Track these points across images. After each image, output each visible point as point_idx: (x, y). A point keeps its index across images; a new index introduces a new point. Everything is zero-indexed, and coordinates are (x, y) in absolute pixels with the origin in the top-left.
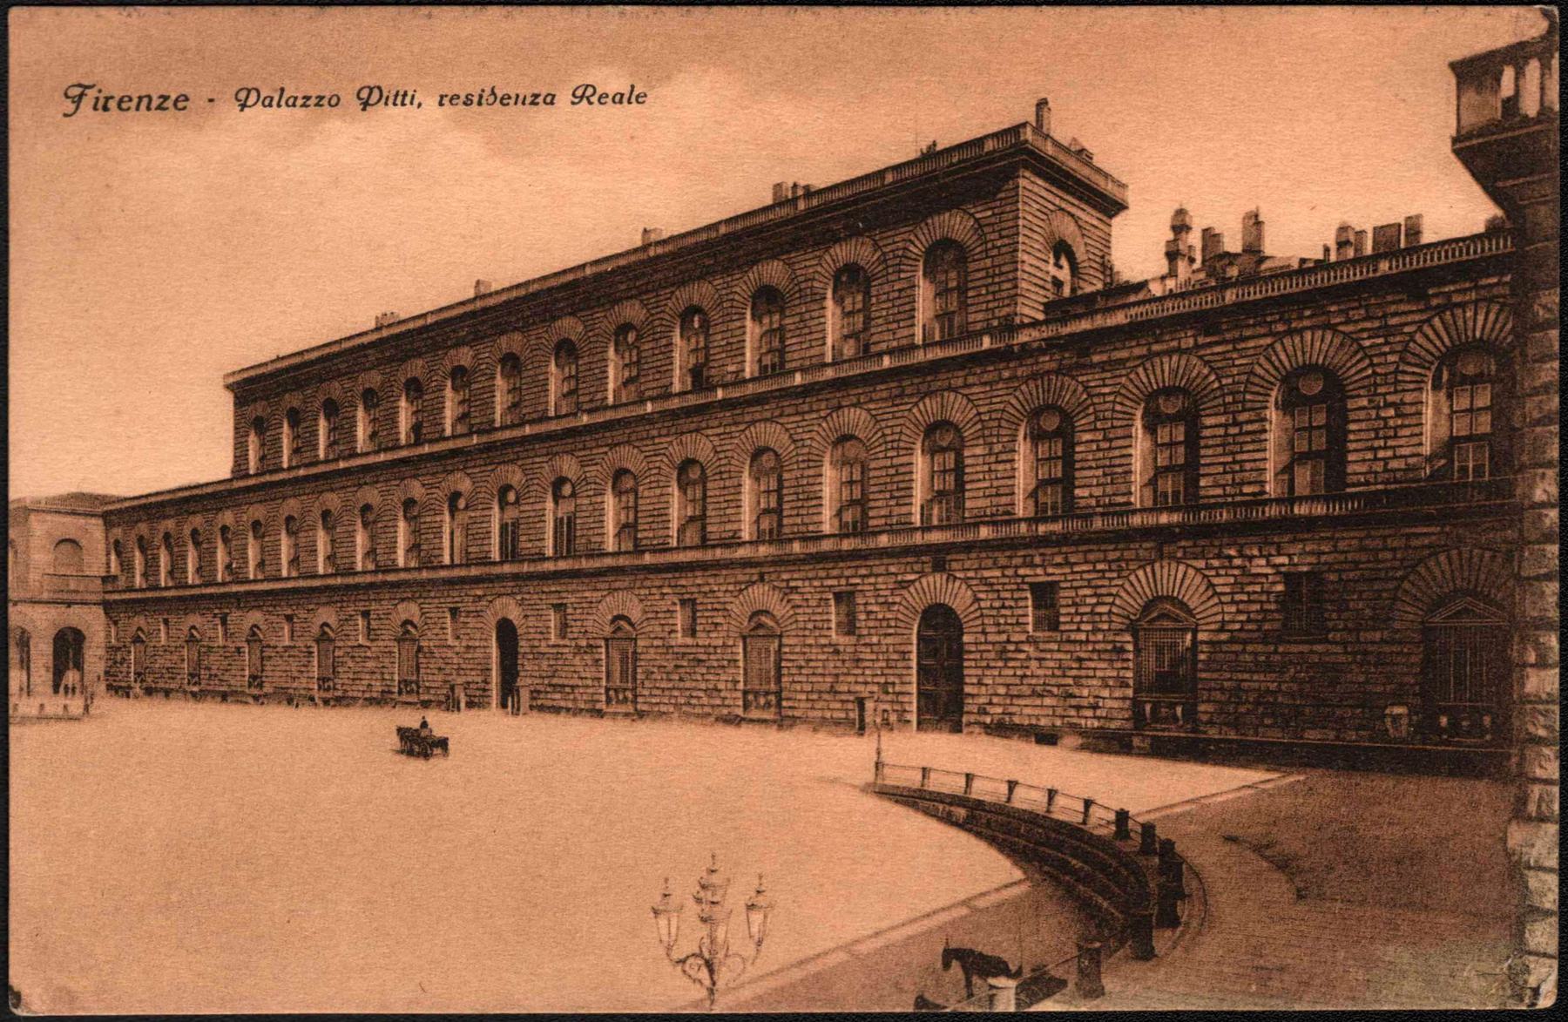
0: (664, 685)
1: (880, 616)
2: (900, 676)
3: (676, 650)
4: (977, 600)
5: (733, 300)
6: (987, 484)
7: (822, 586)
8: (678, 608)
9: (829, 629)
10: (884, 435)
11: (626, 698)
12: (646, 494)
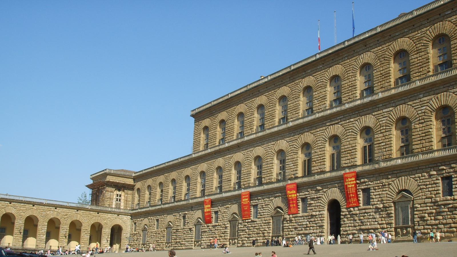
0: (433, 222)
3: (440, 203)
8: (440, 181)
11: (408, 233)
12: (417, 126)
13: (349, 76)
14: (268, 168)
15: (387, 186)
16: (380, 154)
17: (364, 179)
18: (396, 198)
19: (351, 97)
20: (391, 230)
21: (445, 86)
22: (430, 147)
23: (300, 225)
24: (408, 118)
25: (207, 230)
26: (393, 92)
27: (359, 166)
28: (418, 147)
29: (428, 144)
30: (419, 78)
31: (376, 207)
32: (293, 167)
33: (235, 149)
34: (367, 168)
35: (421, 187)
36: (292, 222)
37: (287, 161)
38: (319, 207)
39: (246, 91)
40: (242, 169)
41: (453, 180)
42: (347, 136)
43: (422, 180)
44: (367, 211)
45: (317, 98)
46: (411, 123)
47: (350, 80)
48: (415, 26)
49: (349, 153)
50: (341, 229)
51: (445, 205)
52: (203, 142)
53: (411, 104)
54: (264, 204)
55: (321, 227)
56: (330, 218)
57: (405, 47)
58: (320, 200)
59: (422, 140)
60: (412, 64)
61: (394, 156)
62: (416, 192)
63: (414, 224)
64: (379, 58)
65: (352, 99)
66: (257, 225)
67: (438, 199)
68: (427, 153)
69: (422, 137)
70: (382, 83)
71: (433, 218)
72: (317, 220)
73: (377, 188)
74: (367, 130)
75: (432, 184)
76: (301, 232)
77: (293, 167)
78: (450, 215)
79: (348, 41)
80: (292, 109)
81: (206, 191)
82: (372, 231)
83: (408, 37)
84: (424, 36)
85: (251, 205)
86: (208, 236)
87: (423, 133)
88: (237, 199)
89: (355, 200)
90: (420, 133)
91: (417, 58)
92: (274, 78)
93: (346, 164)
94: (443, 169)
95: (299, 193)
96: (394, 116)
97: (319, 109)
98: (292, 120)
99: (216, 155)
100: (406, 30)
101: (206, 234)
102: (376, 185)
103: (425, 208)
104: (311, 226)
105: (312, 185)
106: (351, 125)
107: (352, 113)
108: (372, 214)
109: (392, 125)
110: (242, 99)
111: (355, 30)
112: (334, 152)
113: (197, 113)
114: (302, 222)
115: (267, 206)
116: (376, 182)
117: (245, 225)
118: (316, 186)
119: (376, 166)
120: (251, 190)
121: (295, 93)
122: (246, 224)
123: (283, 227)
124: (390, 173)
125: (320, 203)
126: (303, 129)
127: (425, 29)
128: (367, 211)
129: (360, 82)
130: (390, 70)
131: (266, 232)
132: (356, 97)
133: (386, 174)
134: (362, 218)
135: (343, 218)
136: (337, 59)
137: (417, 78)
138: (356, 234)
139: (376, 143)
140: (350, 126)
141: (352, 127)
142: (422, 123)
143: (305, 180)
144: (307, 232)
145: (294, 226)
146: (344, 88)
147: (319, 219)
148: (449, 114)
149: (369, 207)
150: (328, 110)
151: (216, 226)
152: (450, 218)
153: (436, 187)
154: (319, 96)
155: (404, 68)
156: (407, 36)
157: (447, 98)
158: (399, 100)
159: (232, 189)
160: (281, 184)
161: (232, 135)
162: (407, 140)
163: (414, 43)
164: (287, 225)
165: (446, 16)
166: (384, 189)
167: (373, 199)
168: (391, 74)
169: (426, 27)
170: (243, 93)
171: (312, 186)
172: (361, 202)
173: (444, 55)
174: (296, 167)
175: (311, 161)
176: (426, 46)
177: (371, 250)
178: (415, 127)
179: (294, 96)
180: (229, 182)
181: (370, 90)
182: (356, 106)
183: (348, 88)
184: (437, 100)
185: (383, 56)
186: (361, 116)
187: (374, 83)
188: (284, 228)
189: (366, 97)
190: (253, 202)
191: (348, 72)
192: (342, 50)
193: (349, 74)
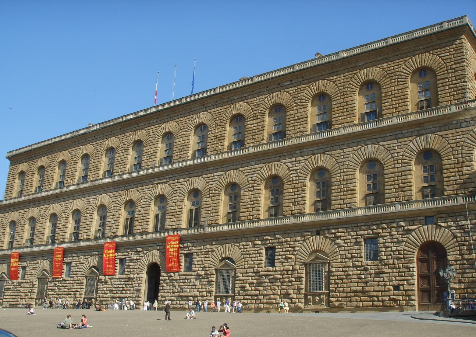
1: (394, 249)
2: (407, 280)
3: (261, 273)
4: (455, 237)
5: (301, 99)
6: (456, 178)
7: (357, 235)
8: (264, 251)
9: (361, 257)
10: (393, 157)
12: (246, 193)
13: (183, 134)
14: (87, 223)
15: (210, 253)
16: (205, 219)
17: (187, 243)
18: (218, 265)
19: (182, 156)
20: (210, 298)
21: (277, 156)
22: (257, 216)
23: (116, 288)
24: (238, 184)
25: (11, 287)
26: (226, 156)
27: (184, 229)
28: (245, 215)
29: (255, 213)
30: (253, 145)
31: (197, 274)
32: (114, 225)
33: (53, 200)
34: (191, 232)
35: (245, 256)
36: (108, 283)
37: (108, 217)
38: (137, 269)
39: (72, 137)
40: (58, 222)
41: (277, 250)
42: (174, 197)
43: (246, 248)
44: (187, 277)
45: (146, 154)
46: (240, 189)
47: (184, 139)
48: (255, 92)
49: (174, 215)
50: (159, 294)
51: (266, 276)
52: (17, 188)
53: (242, 170)
54: (78, 262)
55: (138, 291)
56: (148, 282)
57: (243, 112)
58: (139, 262)
59: (250, 208)
60: (247, 130)
61: (220, 222)
62: (239, 261)
63: (234, 293)
64: (215, 119)
65: (183, 159)
66: (69, 285)
67: (260, 269)
68: (253, 222)
69: (251, 205)
70: (216, 145)
71: (253, 288)
72: (135, 284)
73: (200, 253)
74: (195, 193)
75: (255, 254)
76: (117, 295)
77: (114, 225)
78: (270, 286)
79: (186, 98)
80: (119, 163)
81: (14, 244)
82: (192, 298)
83: (246, 103)
84: (262, 104)
85: (64, 262)
86: (11, 294)
87: (252, 201)
88: (49, 255)
89: (176, 264)
90: (248, 200)
91: (253, 124)
92: (104, 128)
93: (170, 226)
94: (268, 240)
95: (118, 253)
96: (224, 181)
97: (147, 166)
98: (117, 174)
99: (30, 204)
100: (245, 95)
101: (10, 291)
102: (199, 251)
103: (247, 278)
104: (127, 290)
105: (132, 246)
106: (179, 186)
107: (182, 173)
108: (192, 280)
109: (221, 190)
110: (67, 146)
111: (194, 88)
112: (159, 212)
113: (14, 156)
114: (118, 285)
115: (81, 265)
116: (200, 248)
117: (55, 284)
118: (137, 246)
119: (202, 231)
120: (65, 246)
121: (124, 146)
122: (57, 283)
123: (97, 288)
124: (215, 239)
125: (139, 265)
126: (127, 185)
127: (264, 96)
128: (187, 277)
129: (193, 142)
130: (225, 133)
131: (78, 293)
132: (188, 157)
133: (211, 239)
134: (182, 284)
135: (162, 283)
136: (172, 116)
137: (251, 145)
138: (174, 300)
139: (203, 206)
140: (178, 186)
141: (180, 188)
142: (251, 191)
143: (126, 239)
144: (122, 295)
145: (109, 288)
146: (177, 146)
147: (136, 282)
148: (279, 184)
149: (190, 273)
150: (157, 167)
151: (22, 283)
152: (270, 290)
153: (259, 257)
154: (149, 152)
155: (239, 133)
156: (245, 101)
157: (278, 168)
158: (231, 164)
159: (44, 243)
160: (99, 242)
161: (50, 183)
162: (235, 207)
163: (252, 109)
164: (101, 287)
165: (284, 87)
166: (207, 256)
167: (195, 265)
168: (225, 138)
169: (265, 95)
170: (68, 139)
171: (132, 247)
172: (183, 267)
173: (279, 124)
174: (117, 224)
175: (134, 220)
176: (263, 113)
177: (188, 318)
178: (244, 194)
179: (122, 149)
180: (42, 235)
181: (203, 152)
182: (186, 167)
183: (180, 147)
184: (268, 168)
185: (219, 118)
186: (191, 177)
187: (208, 144)
188: (98, 289)
189: (198, 158)
190: (67, 260)
191: (182, 130)
192: (180, 107)
193: (183, 132)
